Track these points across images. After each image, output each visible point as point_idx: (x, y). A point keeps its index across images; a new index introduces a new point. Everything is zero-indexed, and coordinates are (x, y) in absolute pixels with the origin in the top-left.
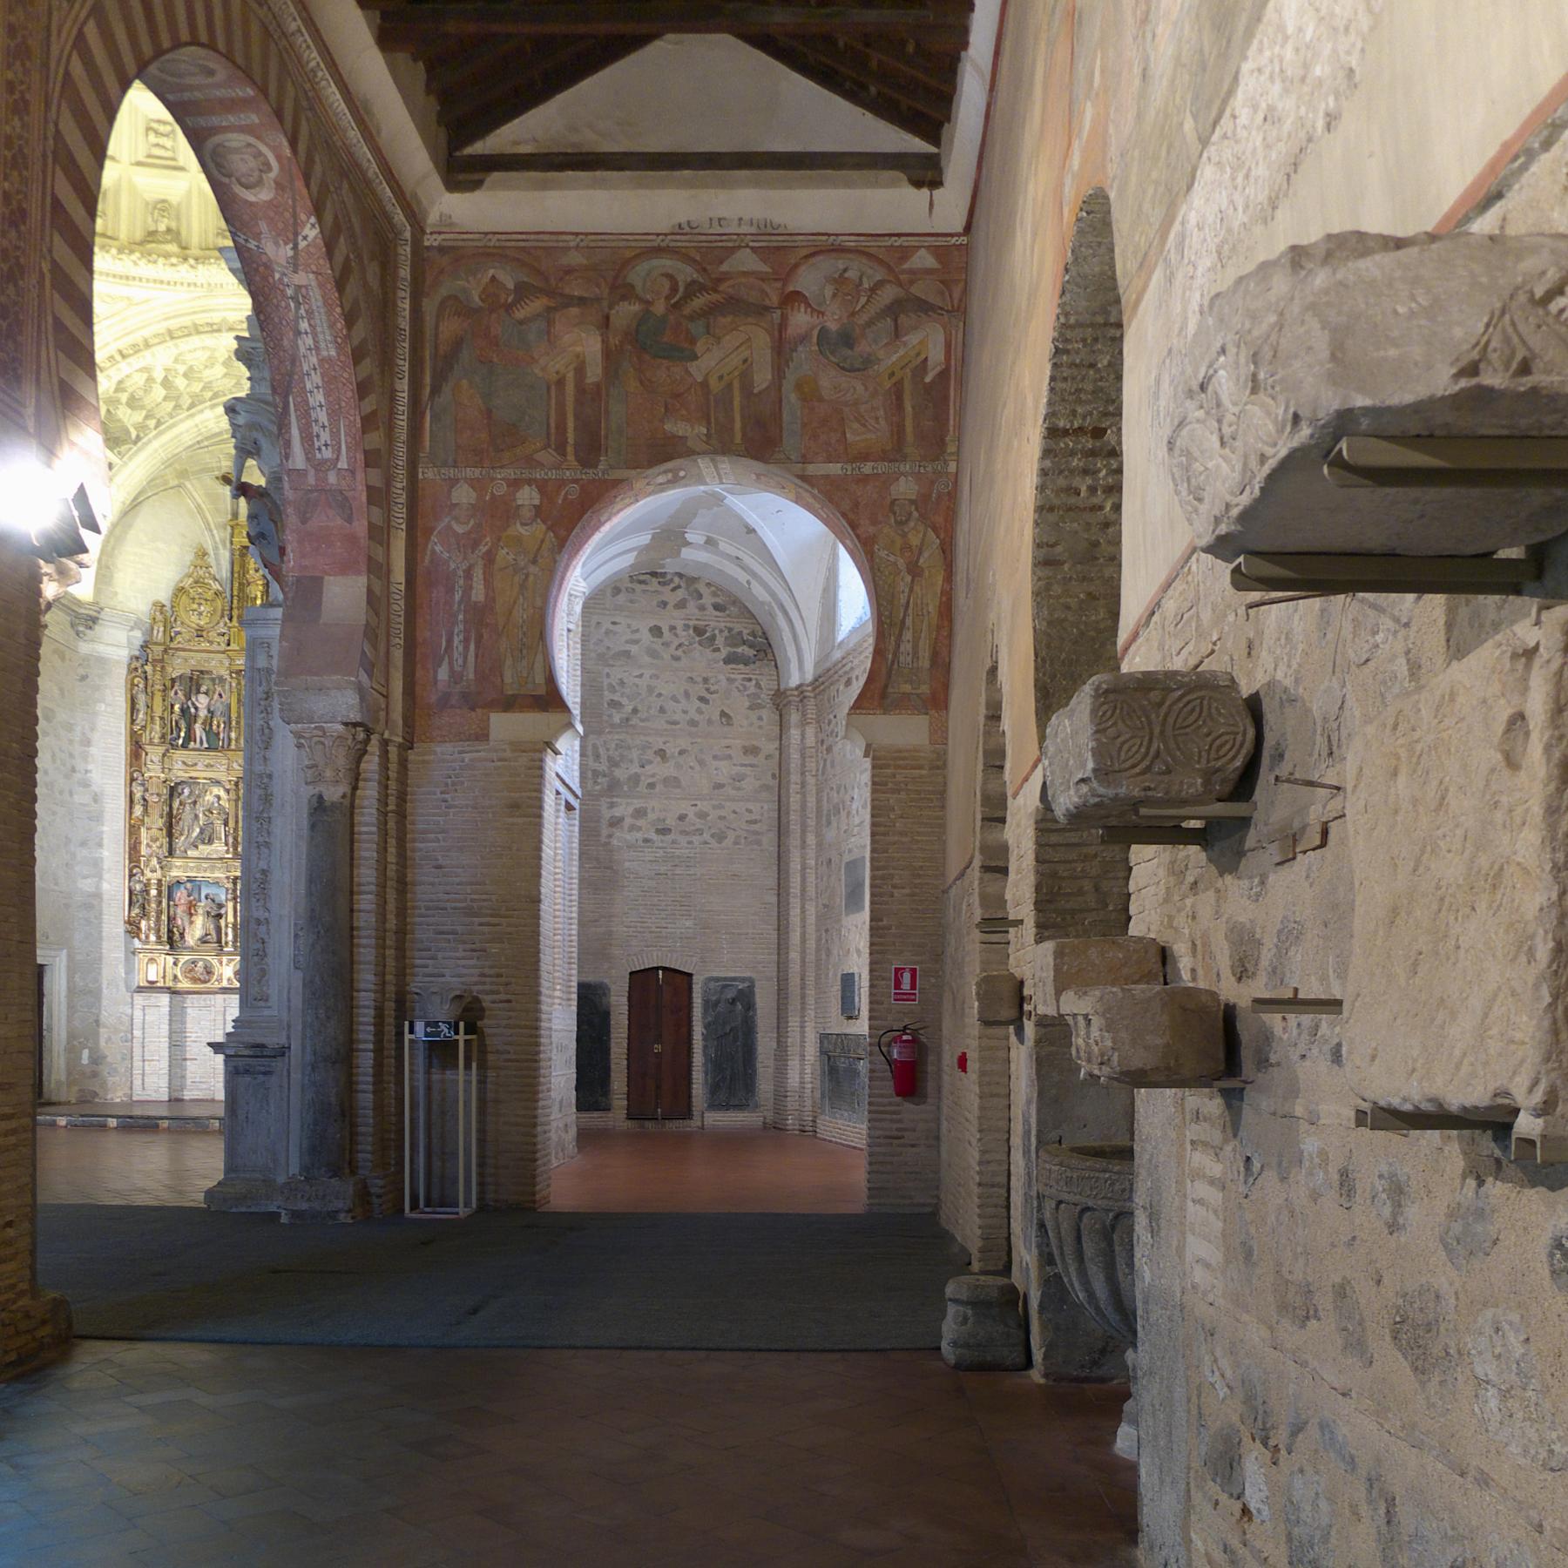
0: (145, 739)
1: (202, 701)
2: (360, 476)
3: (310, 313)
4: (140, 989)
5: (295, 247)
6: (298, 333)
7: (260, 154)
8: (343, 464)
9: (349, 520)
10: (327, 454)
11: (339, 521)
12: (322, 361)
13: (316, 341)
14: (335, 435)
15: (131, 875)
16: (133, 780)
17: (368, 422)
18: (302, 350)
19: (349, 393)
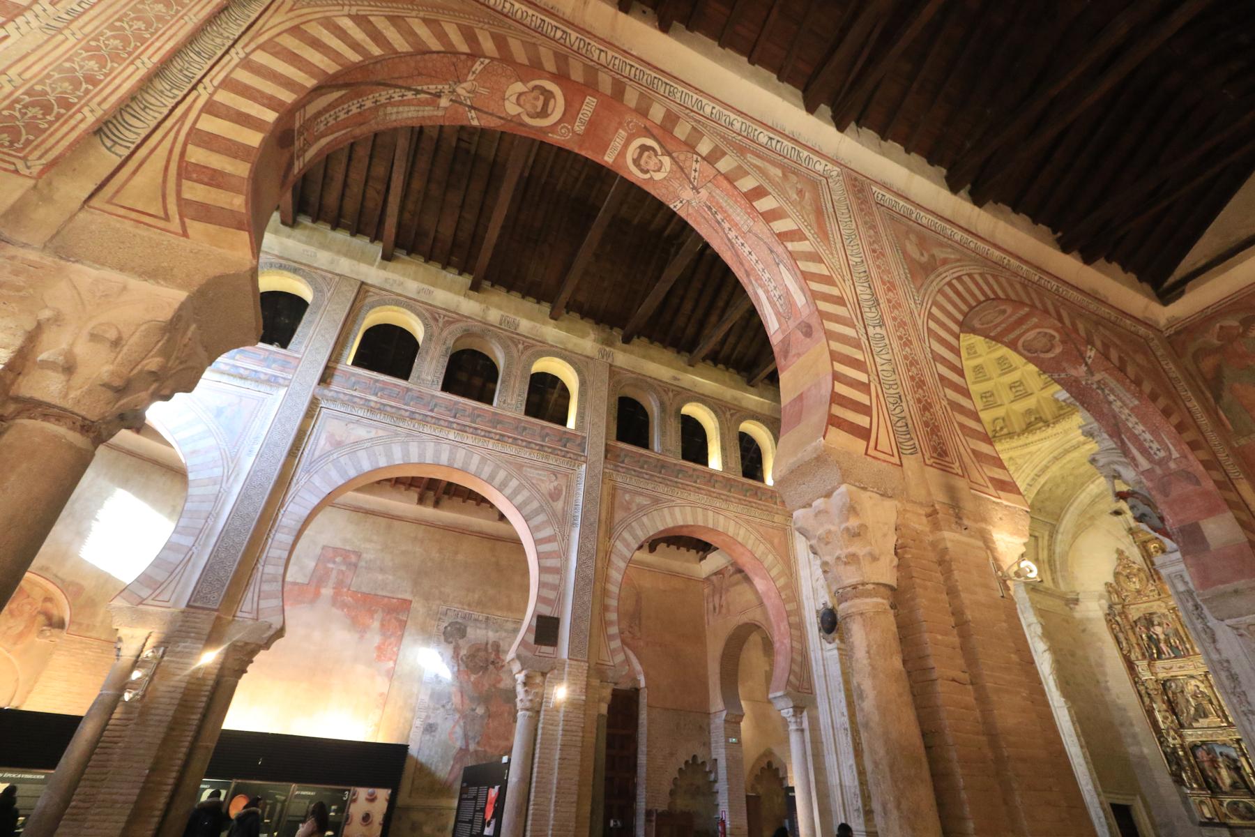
0: (1133, 657)
2: (1191, 457)
3: (1112, 391)
5: (1086, 364)
6: (1110, 403)
7: (1046, 333)
8: (1175, 455)
9: (1198, 482)
10: (1162, 454)
11: (1191, 487)
12: (1132, 409)
13: (1123, 402)
14: (1161, 442)
17: (1180, 428)
18: (1117, 410)
19: (1158, 419)
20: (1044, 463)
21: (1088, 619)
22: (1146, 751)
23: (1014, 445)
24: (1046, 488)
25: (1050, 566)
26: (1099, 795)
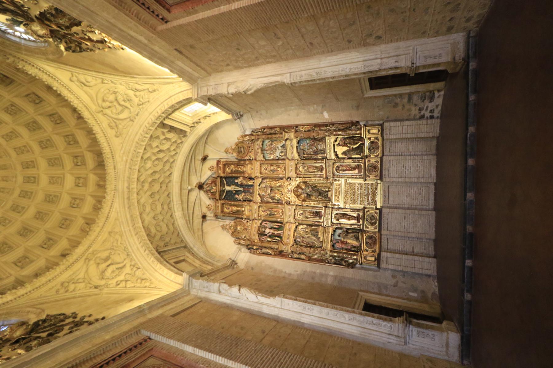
1: (268, 231)
4: (379, 266)
15: (328, 263)
16: (292, 258)
20: (128, 216)
21: (248, 262)
22: (331, 273)
23: (101, 224)
24: (153, 230)
25: (204, 263)
26: (354, 312)
